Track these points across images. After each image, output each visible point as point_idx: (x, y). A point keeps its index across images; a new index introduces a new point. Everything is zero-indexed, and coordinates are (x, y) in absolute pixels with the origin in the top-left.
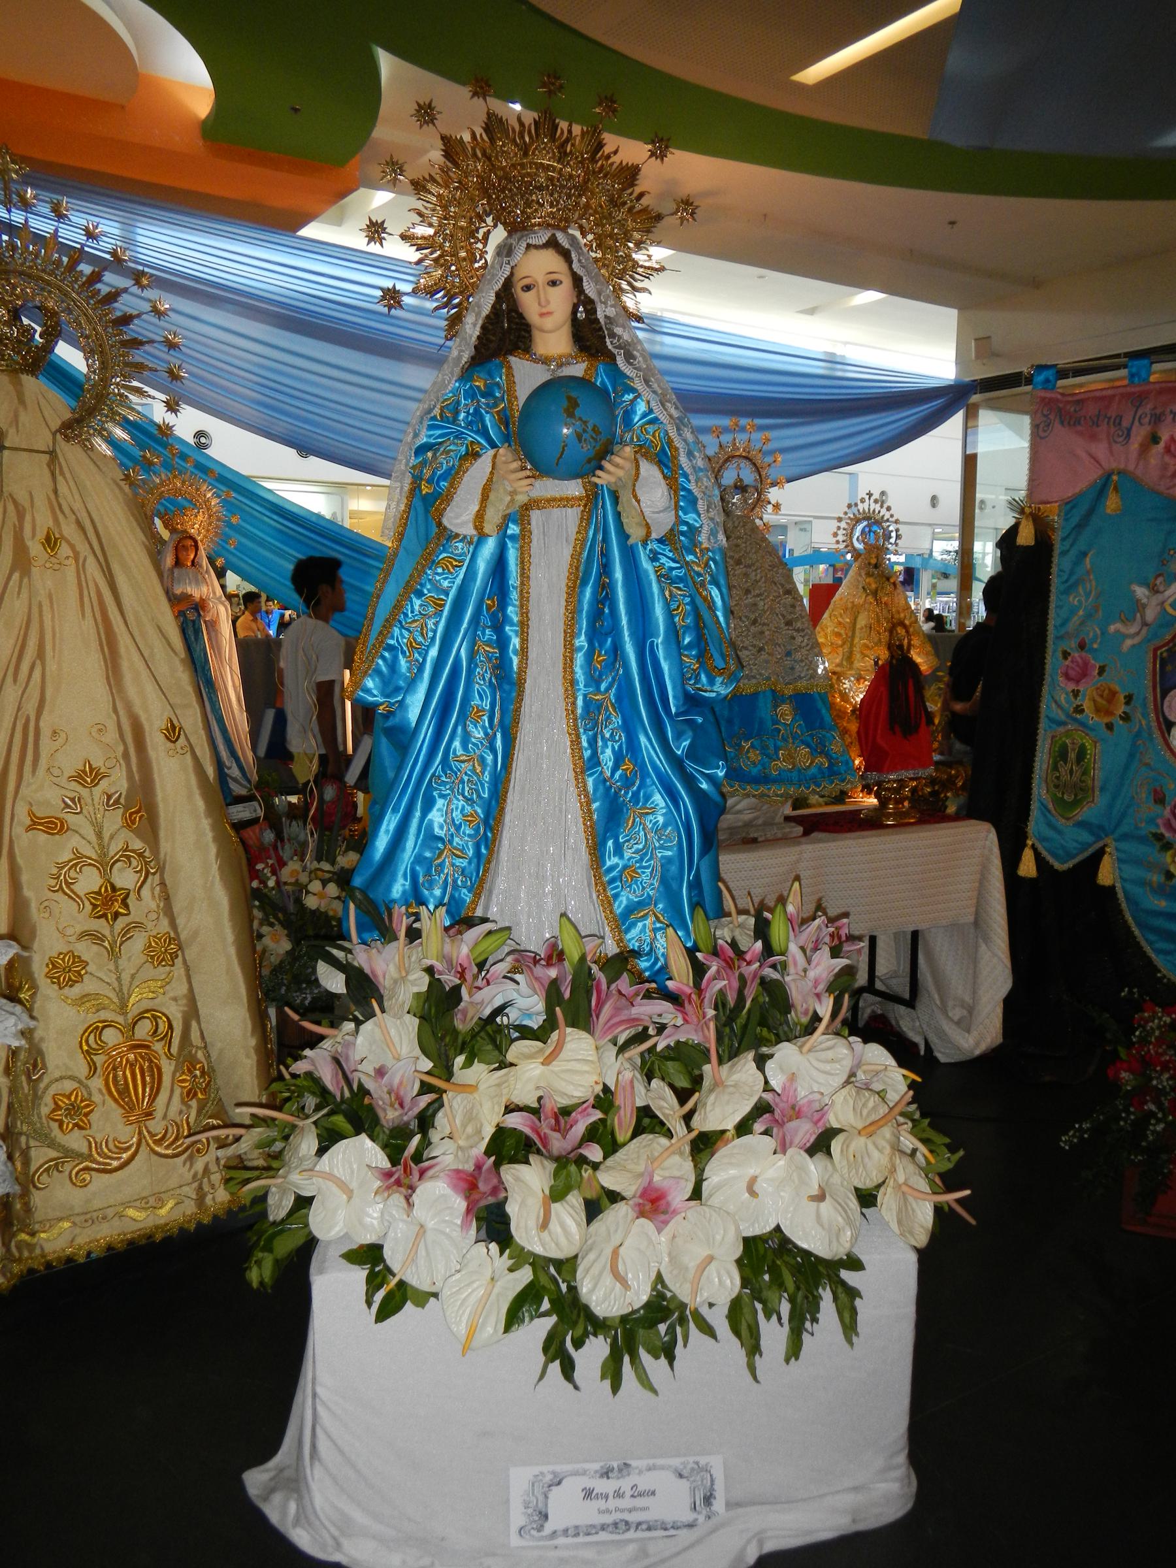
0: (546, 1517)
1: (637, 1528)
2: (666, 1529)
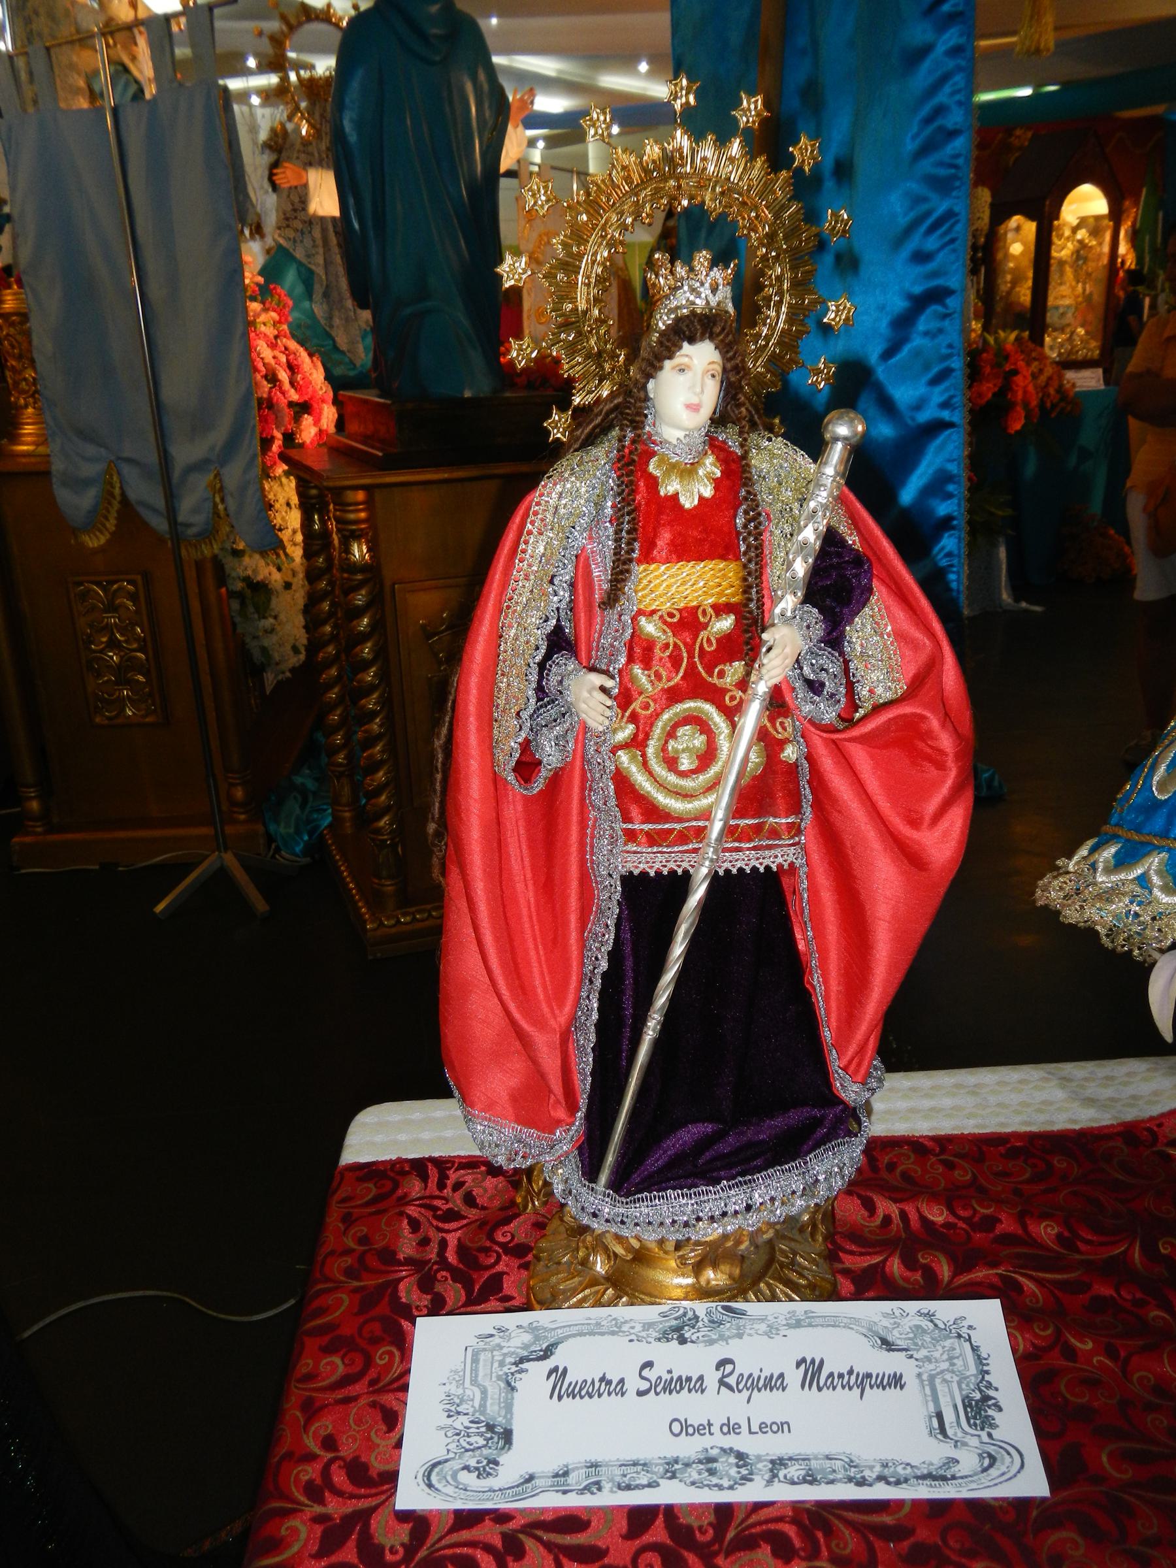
0: (507, 1437)
1: (775, 1476)
2: (862, 1483)
